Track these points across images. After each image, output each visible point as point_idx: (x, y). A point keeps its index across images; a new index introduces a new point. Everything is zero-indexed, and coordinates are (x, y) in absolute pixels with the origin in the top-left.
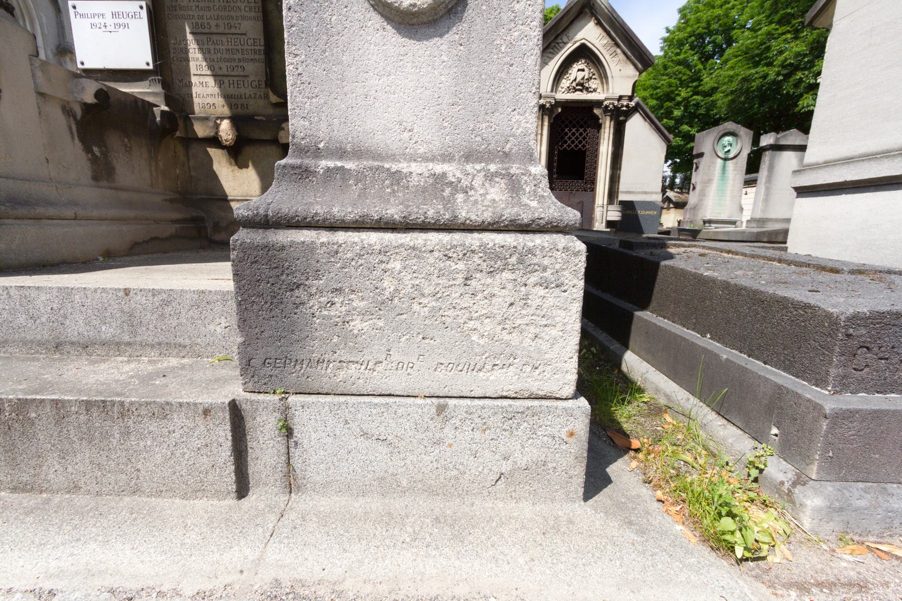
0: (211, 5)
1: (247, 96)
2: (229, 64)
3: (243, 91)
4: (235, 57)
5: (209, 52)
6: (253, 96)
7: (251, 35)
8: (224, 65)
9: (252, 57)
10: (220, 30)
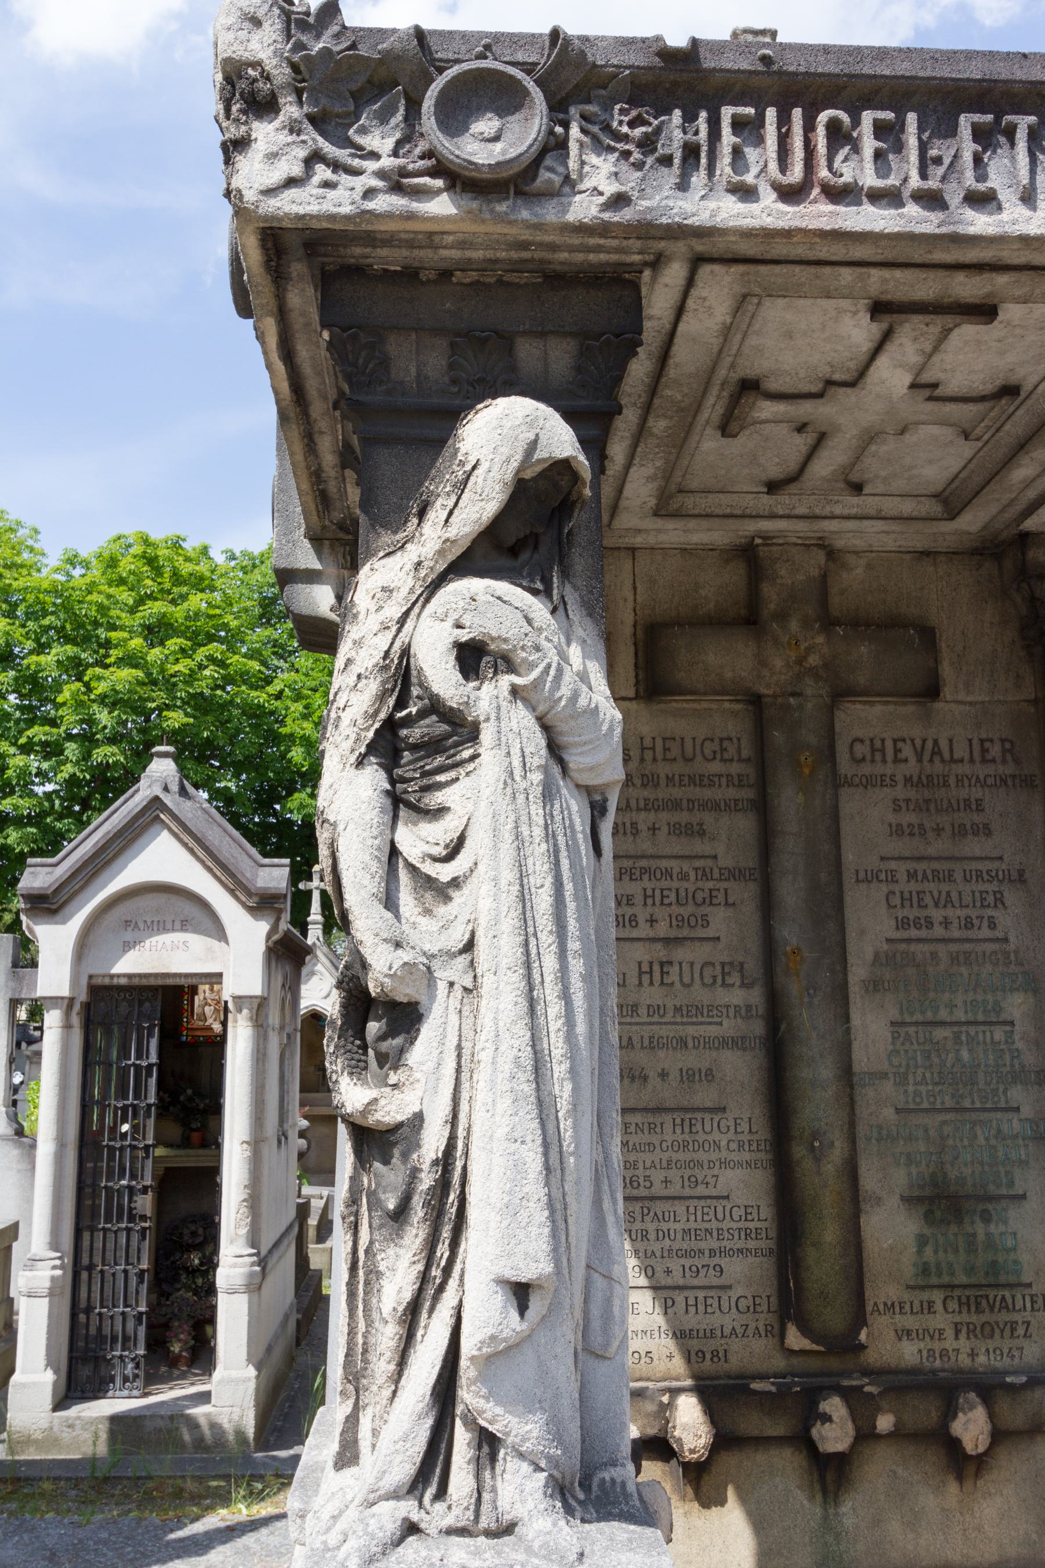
0: (655, 1140)
1: (727, 1331)
2: (687, 1262)
3: (716, 1320)
4: (703, 1245)
5: (645, 1235)
6: (740, 1331)
7: (741, 1198)
8: (675, 1265)
9: (741, 1244)
10: (674, 1190)
